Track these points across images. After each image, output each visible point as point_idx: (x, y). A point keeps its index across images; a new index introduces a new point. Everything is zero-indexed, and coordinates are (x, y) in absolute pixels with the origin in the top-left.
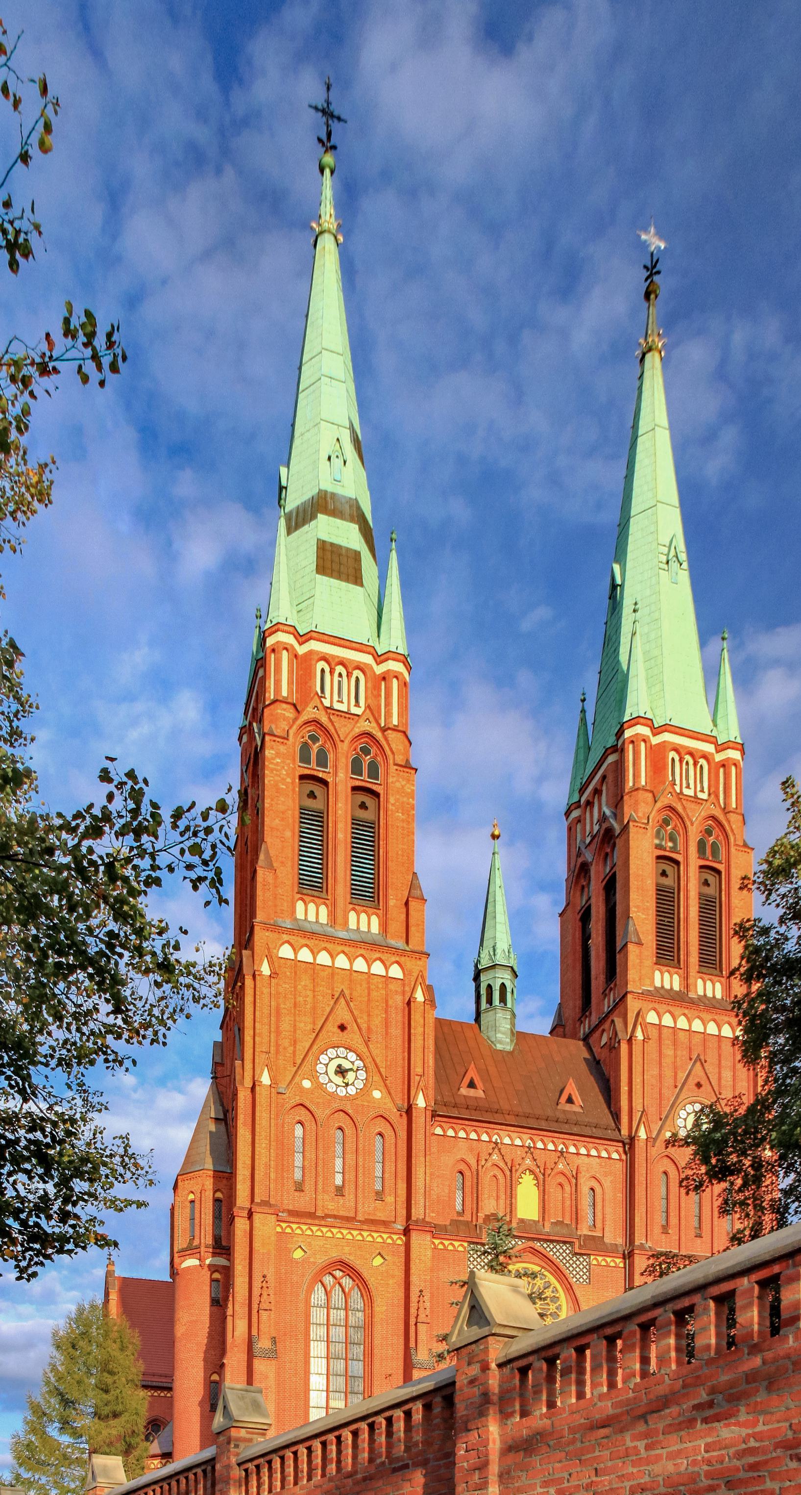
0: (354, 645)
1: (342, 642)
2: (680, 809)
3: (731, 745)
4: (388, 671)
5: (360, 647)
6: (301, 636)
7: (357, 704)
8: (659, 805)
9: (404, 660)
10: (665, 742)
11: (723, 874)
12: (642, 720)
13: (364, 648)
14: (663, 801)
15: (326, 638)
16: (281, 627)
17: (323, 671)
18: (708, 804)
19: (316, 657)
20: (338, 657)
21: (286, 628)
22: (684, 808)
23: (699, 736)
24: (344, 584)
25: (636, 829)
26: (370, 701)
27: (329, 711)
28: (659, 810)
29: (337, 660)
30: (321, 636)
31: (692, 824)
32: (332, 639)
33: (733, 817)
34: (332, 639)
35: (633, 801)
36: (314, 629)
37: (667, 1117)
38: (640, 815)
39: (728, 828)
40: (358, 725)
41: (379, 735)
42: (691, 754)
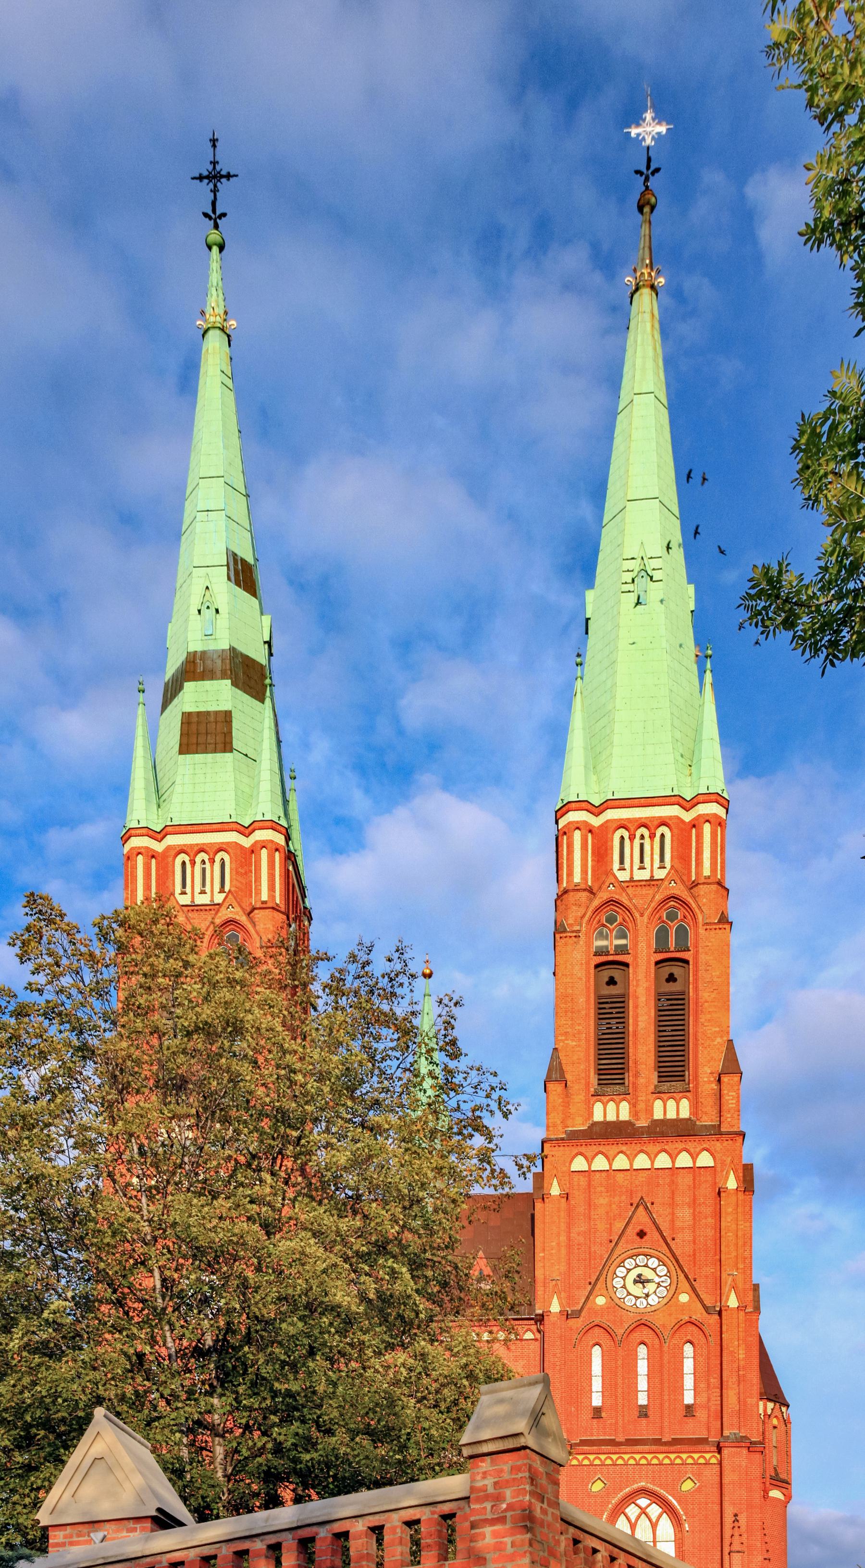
0: (214, 827)
1: (201, 827)
2: (625, 900)
3: (701, 798)
4: (256, 842)
5: (222, 827)
6: (159, 833)
7: (222, 891)
8: (596, 903)
9: (273, 826)
10: (607, 821)
11: (691, 963)
12: (573, 805)
13: (226, 827)
14: (603, 896)
15: (183, 828)
16: (133, 832)
17: (184, 863)
18: (666, 883)
19: (173, 853)
20: (197, 845)
21: (138, 832)
22: (630, 900)
23: (654, 801)
24: (210, 756)
25: (563, 941)
26: (234, 882)
27: (185, 909)
28: (597, 910)
29: (196, 849)
30: (177, 829)
31: (642, 915)
32: (189, 828)
33: (702, 890)
34: (189, 828)
35: (564, 906)
36: (169, 823)
37: (597, 1279)
38: (571, 921)
39: (694, 905)
40: (220, 914)
41: (243, 919)
42: (645, 826)
